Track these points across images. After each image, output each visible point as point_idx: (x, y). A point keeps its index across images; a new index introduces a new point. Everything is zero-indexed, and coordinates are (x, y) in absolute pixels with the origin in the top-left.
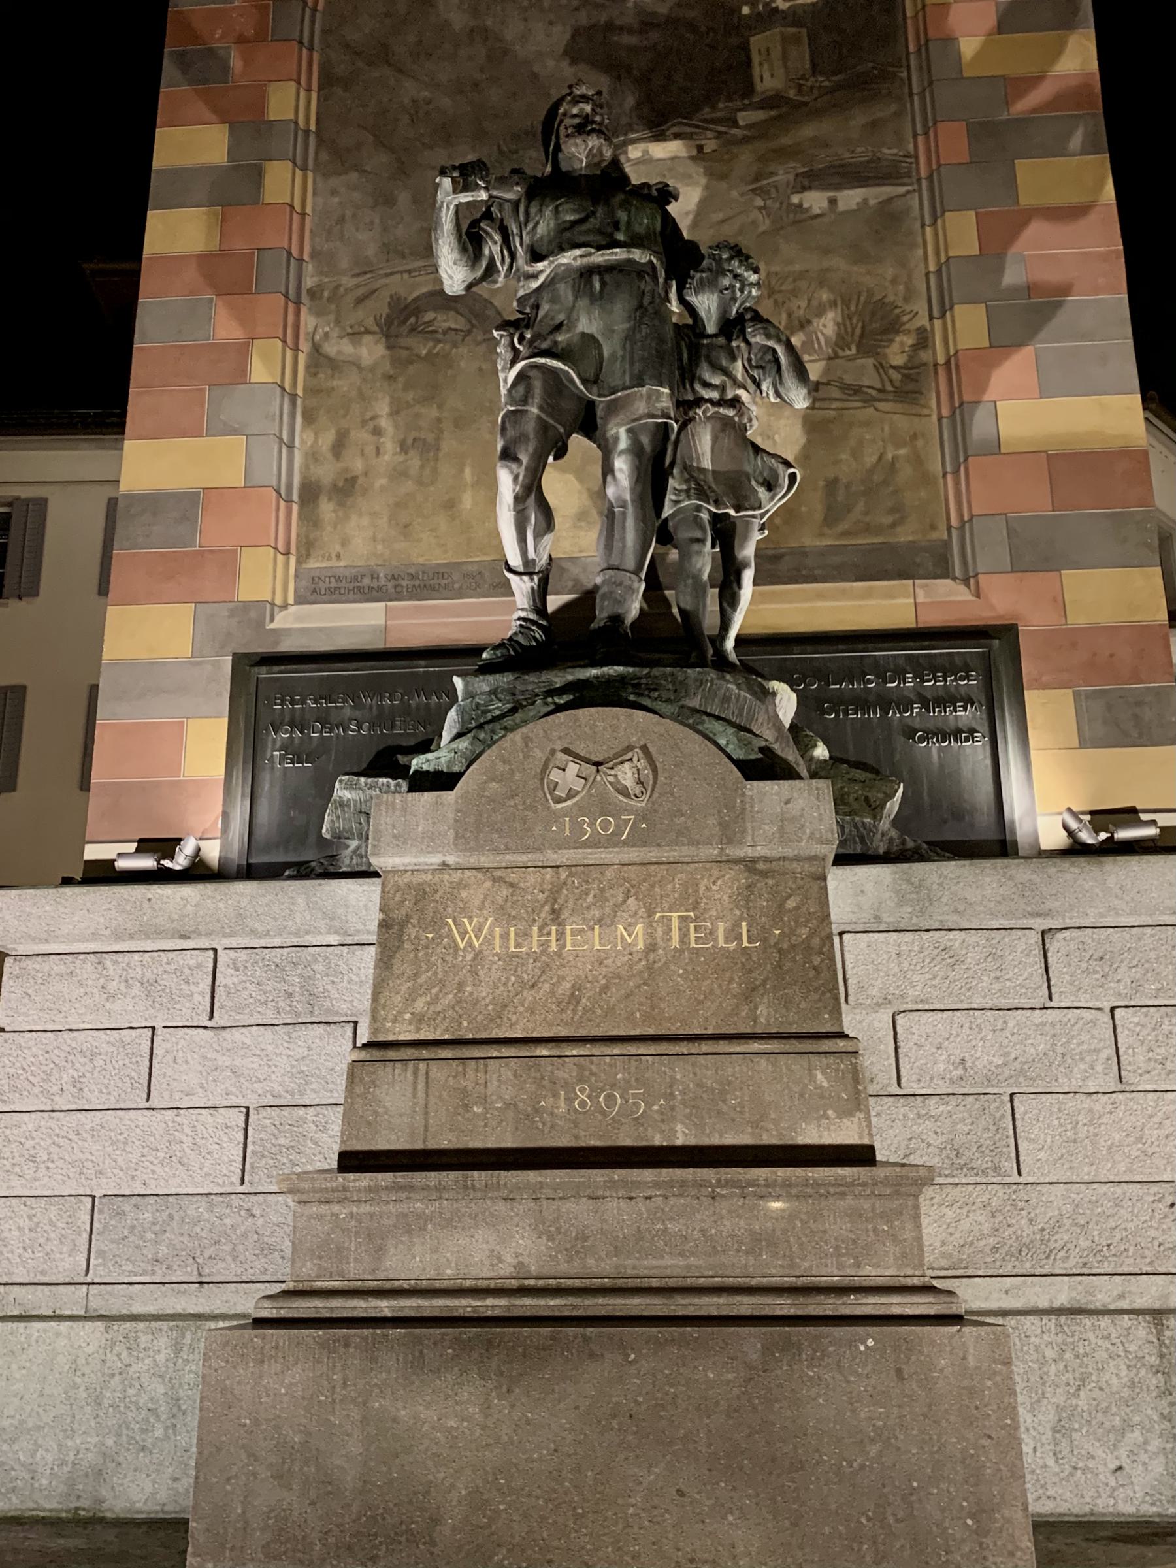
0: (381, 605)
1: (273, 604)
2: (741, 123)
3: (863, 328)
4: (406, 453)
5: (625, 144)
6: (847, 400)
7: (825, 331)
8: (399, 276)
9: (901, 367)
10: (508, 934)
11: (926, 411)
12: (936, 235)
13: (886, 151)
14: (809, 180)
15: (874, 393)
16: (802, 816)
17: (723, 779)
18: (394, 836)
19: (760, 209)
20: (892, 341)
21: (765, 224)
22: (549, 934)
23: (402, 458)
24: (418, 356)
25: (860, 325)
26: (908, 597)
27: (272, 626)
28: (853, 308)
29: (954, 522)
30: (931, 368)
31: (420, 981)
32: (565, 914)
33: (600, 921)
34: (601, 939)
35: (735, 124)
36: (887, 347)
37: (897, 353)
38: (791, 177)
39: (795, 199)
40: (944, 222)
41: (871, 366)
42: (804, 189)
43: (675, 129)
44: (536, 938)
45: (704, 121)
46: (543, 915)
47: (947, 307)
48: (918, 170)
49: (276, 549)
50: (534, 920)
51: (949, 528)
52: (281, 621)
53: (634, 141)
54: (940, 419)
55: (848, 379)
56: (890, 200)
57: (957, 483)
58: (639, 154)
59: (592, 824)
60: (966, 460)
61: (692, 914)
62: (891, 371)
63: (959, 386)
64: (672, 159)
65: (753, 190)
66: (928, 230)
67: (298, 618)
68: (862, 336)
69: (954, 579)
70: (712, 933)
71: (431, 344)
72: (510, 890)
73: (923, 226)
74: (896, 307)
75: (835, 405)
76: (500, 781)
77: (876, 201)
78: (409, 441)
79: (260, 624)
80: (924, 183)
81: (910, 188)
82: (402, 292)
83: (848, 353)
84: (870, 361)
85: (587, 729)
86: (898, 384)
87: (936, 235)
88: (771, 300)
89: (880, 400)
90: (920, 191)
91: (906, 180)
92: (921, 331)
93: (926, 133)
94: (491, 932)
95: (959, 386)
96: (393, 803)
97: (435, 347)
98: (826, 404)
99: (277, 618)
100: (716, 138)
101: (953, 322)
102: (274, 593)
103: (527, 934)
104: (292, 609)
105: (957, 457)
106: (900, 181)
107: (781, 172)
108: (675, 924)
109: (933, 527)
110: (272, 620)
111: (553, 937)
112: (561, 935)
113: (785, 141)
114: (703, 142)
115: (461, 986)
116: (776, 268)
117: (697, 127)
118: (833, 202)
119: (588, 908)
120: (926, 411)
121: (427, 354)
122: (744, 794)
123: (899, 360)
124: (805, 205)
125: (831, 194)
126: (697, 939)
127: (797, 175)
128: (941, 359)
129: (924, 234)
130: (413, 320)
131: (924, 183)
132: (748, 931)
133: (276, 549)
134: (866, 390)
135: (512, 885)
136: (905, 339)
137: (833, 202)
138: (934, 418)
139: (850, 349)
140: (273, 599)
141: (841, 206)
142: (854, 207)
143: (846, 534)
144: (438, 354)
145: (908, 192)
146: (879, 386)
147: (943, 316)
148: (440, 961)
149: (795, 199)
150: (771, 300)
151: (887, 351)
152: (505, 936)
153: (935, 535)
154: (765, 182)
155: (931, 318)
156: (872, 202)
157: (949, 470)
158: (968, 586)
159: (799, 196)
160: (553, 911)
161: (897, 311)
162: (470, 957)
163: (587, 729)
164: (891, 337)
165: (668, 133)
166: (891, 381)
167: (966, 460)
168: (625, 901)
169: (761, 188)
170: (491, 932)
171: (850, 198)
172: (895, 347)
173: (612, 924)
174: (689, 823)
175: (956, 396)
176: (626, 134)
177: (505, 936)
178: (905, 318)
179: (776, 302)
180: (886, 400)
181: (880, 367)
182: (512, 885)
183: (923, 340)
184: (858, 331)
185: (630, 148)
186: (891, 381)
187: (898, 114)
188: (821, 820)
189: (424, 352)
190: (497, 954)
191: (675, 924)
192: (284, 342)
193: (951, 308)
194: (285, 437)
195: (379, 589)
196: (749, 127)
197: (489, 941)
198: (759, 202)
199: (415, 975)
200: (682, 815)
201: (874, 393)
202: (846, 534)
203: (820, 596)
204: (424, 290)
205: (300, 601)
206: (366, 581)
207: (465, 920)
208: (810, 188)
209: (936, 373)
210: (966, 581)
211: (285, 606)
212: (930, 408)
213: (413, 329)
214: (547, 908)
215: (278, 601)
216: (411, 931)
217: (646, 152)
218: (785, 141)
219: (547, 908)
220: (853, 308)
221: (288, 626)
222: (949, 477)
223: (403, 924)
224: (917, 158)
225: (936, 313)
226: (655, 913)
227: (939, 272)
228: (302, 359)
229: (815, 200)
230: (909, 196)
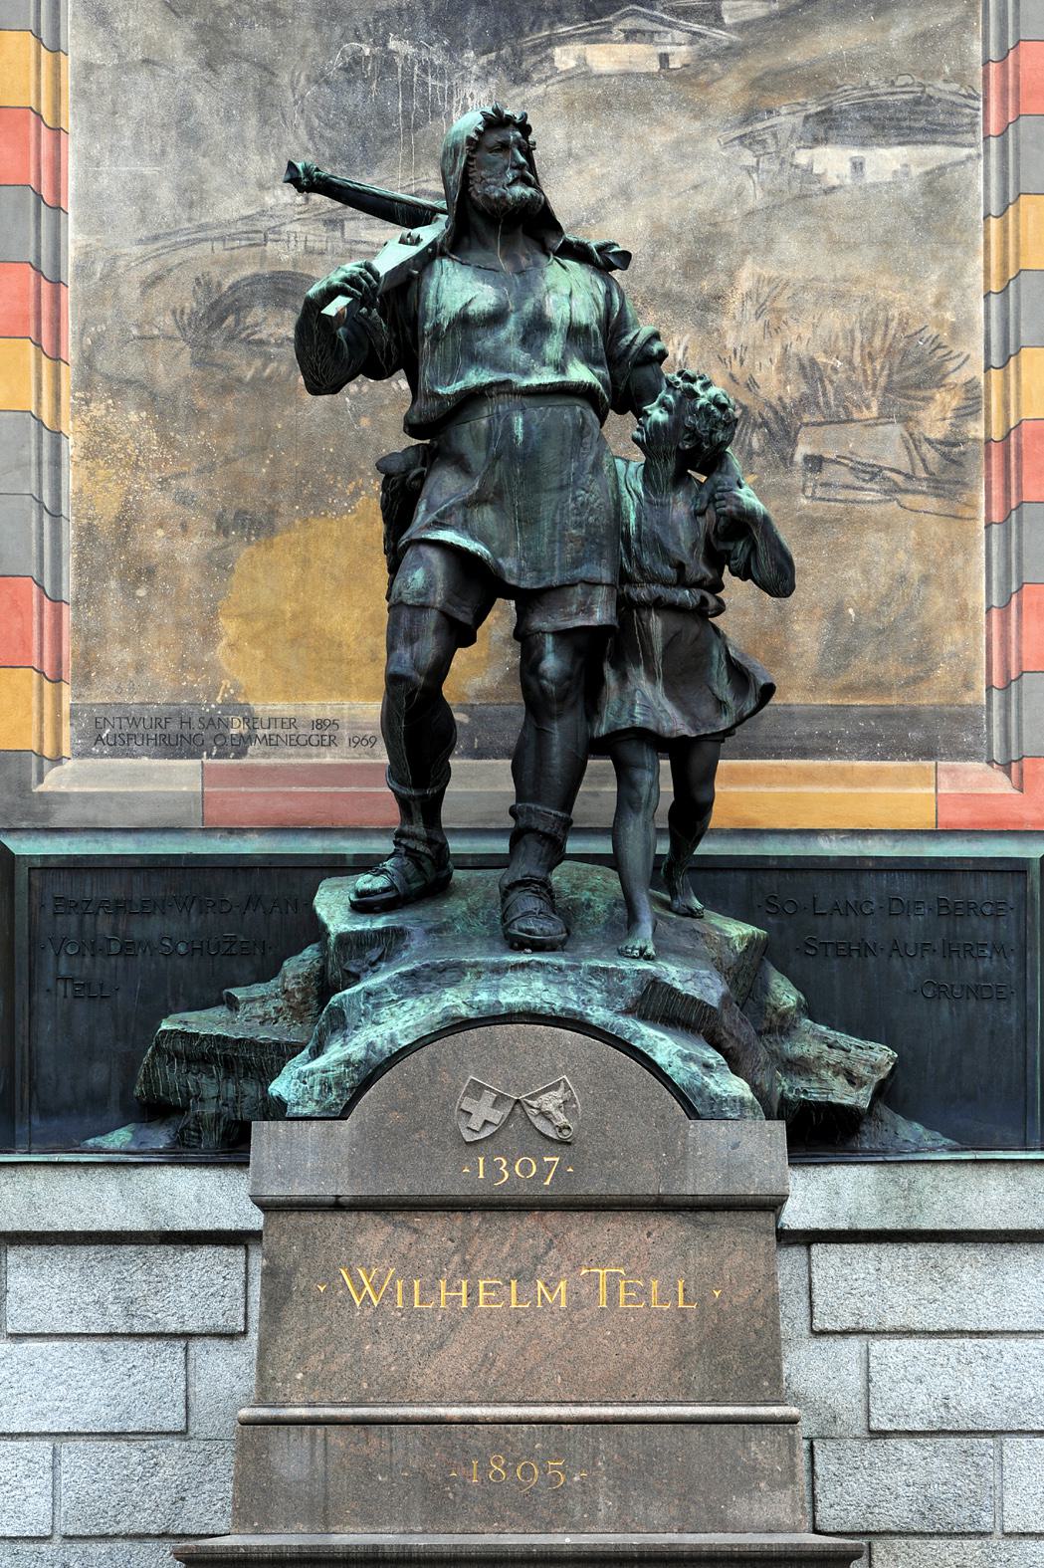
0: (197, 762)
1: (41, 756)
2: (727, 20)
3: (889, 376)
4: (226, 533)
5: (551, 42)
6: (862, 489)
7: (834, 378)
8: (208, 245)
9: (941, 443)
10: (411, 1286)
11: (968, 513)
12: (1005, 230)
13: (940, 84)
14: (826, 126)
15: (899, 478)
16: (751, 1163)
17: (663, 1117)
18: (279, 1173)
19: (749, 170)
20: (929, 399)
21: (755, 197)
22: (459, 1289)
23: (220, 541)
24: (239, 380)
25: (885, 373)
26: (928, 785)
27: (41, 788)
28: (877, 342)
29: (996, 681)
30: (982, 447)
31: (312, 1337)
32: (477, 1266)
33: (517, 1275)
34: (518, 1295)
35: (717, 20)
36: (918, 408)
37: (935, 419)
38: (798, 120)
39: (802, 158)
40: (1018, 210)
41: (898, 440)
42: (817, 141)
43: (629, 24)
44: (443, 1293)
45: (673, 11)
46: (452, 1266)
47: (1012, 352)
48: (986, 120)
49: (41, 673)
50: (443, 1272)
51: (990, 688)
52: (53, 781)
53: (563, 40)
54: (988, 526)
55: (865, 456)
56: (941, 169)
57: (1005, 622)
58: (572, 64)
59: (510, 1167)
60: (1020, 589)
61: (622, 1271)
62: (925, 447)
63: (1019, 478)
64: (626, 75)
65: (741, 138)
66: (994, 223)
67: (77, 778)
68: (887, 389)
69: (990, 762)
70: (644, 1292)
71: (258, 363)
72: (415, 1237)
73: (987, 216)
74: (939, 347)
75: (843, 495)
76: (403, 1110)
77: (921, 170)
78: (230, 516)
79: (24, 787)
80: (994, 143)
81: (973, 151)
82: (215, 273)
83: (866, 414)
84: (895, 430)
85: (505, 1051)
86: (933, 468)
87: (1005, 230)
88: (761, 322)
89: (906, 491)
90: (987, 151)
91: (969, 138)
92: (970, 386)
93: (1003, 59)
94: (393, 1284)
95: (1019, 478)
96: (276, 1132)
97: (265, 366)
98: (832, 494)
99: (47, 778)
100: (691, 43)
101: (1018, 373)
102: (41, 739)
103: (434, 1288)
104: (68, 765)
105: (1008, 583)
106: (959, 139)
107: (784, 110)
108: (603, 1281)
109: (968, 685)
110: (41, 780)
111: (464, 1293)
112: (472, 1292)
113: (796, 55)
114: (668, 49)
115: (358, 1345)
116: (770, 272)
117: (662, 22)
118: (858, 166)
119: (505, 1260)
120: (968, 513)
121: (253, 377)
122: (686, 1136)
123: (938, 432)
124: (816, 171)
125: (855, 153)
126: (628, 1299)
127: (807, 118)
128: (997, 435)
129: (987, 231)
130: (230, 320)
131: (994, 143)
132: (685, 1290)
133: (41, 673)
134: (888, 474)
135: (416, 1231)
136: (948, 398)
137: (858, 166)
138: (982, 523)
139: (868, 407)
140: (41, 748)
141: (870, 176)
142: (888, 178)
143: (849, 689)
144: (270, 378)
145: (969, 158)
146: (907, 469)
147: (1005, 365)
148: (335, 1316)
149: (802, 158)
150: (761, 322)
151: (922, 415)
152: (408, 1291)
153: (968, 699)
154: (759, 126)
155: (988, 367)
156: (916, 171)
157: (995, 603)
158: (1008, 773)
159: (809, 152)
160: (464, 1262)
161: (941, 352)
162: (368, 1312)
163: (505, 1051)
164: (928, 393)
165: (615, 29)
166: (923, 461)
167: (1020, 589)
168: (546, 1253)
169: (751, 135)
170: (393, 1284)
171: (888, 161)
172: (934, 410)
173: (531, 1279)
174: (622, 1167)
175: (1013, 491)
176: (552, 25)
177: (408, 1291)
178: (951, 366)
179: (767, 325)
180: (914, 492)
181: (913, 442)
182: (416, 1231)
183: (972, 403)
184: (882, 381)
185: (557, 51)
186: (923, 461)
187: (964, 23)
188: (772, 1167)
189: (249, 375)
190: (400, 1310)
191: (603, 1281)
192: (38, 345)
193: (1017, 353)
194: (47, 500)
195: (191, 740)
196: (742, 27)
197: (390, 1295)
198: (748, 158)
199: (307, 1330)
200: (614, 1158)
201: (899, 478)
202: (849, 689)
203: (809, 777)
204: (248, 271)
205: (80, 755)
206: (174, 728)
207: (361, 1272)
208: (826, 141)
209: (988, 455)
210: (1006, 767)
211: (58, 760)
212: (975, 507)
213: (231, 338)
214: (456, 1258)
215: (48, 752)
216: (300, 1281)
217: (582, 60)
218: (796, 56)
219: (456, 1258)
220: (877, 342)
221: (63, 789)
222: (995, 612)
223: (291, 1274)
224: (986, 102)
225: (995, 361)
226: (577, 1267)
227: (1005, 291)
228: (68, 375)
229: (832, 161)
230: (969, 165)
